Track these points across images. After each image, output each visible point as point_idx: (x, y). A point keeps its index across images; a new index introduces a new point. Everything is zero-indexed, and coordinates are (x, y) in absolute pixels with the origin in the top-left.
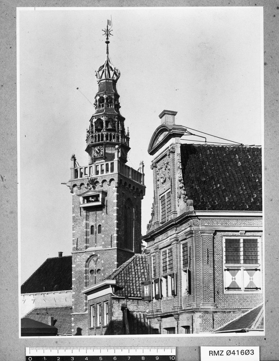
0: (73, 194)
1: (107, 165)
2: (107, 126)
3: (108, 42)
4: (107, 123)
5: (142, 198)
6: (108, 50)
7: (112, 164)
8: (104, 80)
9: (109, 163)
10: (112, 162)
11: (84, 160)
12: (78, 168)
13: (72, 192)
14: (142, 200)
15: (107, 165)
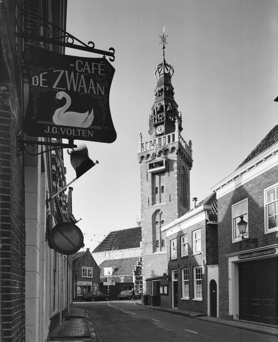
0: (141, 164)
1: (169, 137)
2: (166, 109)
3: (164, 48)
4: (167, 106)
5: (190, 169)
6: (164, 54)
7: (174, 135)
8: (162, 74)
9: (171, 134)
10: (173, 133)
11: (147, 138)
12: (144, 142)
13: (140, 163)
14: (190, 171)
15: (169, 137)
